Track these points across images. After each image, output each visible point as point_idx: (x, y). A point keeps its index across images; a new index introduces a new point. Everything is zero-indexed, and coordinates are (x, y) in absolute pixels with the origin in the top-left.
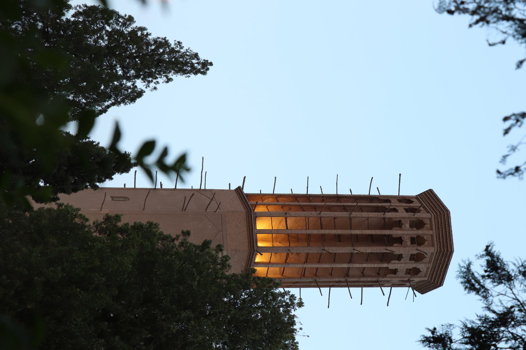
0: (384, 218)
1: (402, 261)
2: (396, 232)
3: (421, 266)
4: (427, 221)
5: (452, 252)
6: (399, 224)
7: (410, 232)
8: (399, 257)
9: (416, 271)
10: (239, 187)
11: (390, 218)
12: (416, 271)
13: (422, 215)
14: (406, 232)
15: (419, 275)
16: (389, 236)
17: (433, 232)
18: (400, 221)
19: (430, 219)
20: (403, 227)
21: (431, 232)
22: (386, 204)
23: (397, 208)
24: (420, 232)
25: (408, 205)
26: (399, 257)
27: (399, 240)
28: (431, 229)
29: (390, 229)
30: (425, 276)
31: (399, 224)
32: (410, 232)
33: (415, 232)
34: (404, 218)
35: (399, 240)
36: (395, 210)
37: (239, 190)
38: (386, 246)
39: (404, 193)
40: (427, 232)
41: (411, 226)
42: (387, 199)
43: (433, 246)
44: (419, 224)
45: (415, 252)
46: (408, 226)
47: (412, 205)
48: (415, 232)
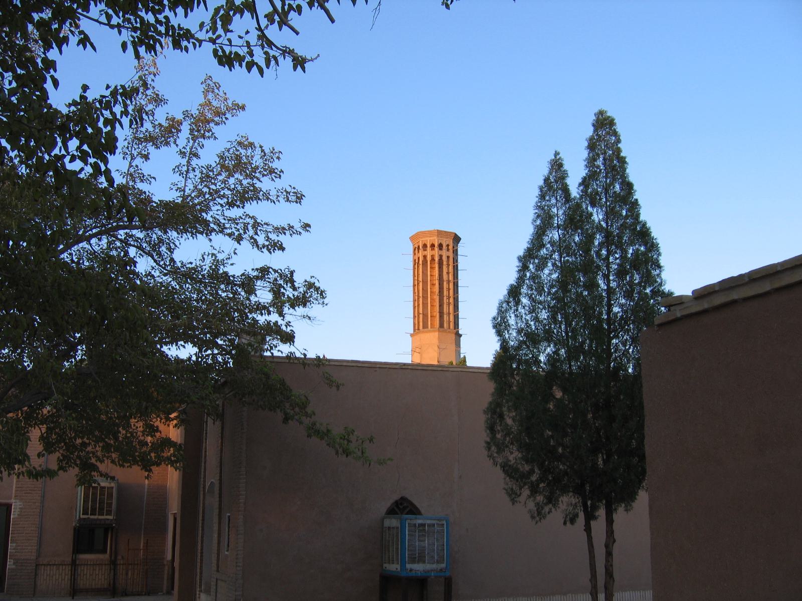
2: (429, 258)
6: (425, 257)
7: (429, 251)
14: (429, 253)
17: (428, 239)
18: (424, 256)
21: (429, 240)
24: (428, 246)
28: (427, 240)
31: (425, 257)
32: (429, 251)
33: (429, 248)
41: (426, 250)
44: (425, 246)
46: (426, 252)
48: (429, 248)
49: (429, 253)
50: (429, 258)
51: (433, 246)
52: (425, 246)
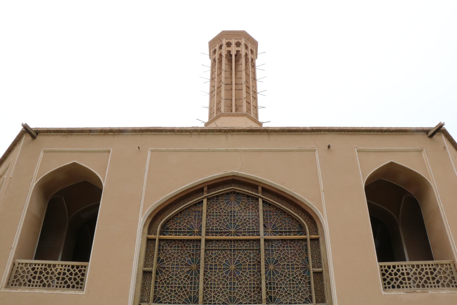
0: (226, 58)
2: (233, 53)
4: (228, 41)
5: (244, 31)
8: (246, 55)
10: (205, 124)
11: (226, 55)
13: (224, 42)
14: (234, 48)
15: (253, 50)
16: (236, 55)
19: (226, 39)
20: (230, 50)
26: (246, 55)
29: (231, 56)
30: (254, 48)
31: (229, 52)
33: (233, 45)
35: (238, 51)
43: (241, 39)
44: (229, 44)
48: (233, 45)
50: (233, 53)
52: (229, 44)
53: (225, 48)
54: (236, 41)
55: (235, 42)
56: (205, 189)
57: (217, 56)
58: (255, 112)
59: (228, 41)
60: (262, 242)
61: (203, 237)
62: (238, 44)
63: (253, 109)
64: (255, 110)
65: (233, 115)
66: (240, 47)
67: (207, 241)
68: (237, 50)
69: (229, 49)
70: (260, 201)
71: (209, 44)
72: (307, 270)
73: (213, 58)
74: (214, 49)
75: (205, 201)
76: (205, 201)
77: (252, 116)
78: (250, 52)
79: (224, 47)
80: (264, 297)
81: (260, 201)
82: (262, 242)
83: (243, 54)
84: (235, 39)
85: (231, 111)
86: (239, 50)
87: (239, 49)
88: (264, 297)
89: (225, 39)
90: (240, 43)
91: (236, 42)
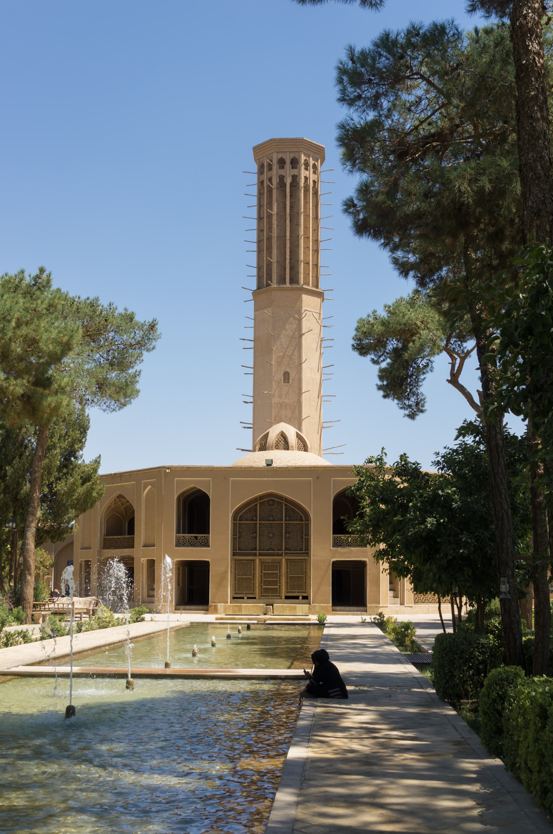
0: (277, 188)
1: (308, 176)
2: (288, 181)
3: (312, 162)
4: (280, 156)
6: (282, 178)
8: (306, 178)
9: (315, 166)
10: (253, 293)
11: (277, 184)
12: (315, 166)
14: (288, 172)
15: (316, 163)
16: (291, 186)
19: (278, 153)
20: (283, 174)
22: (265, 185)
23: (269, 176)
24: (288, 161)
25: (265, 168)
26: (306, 178)
27: (295, 179)
29: (285, 184)
31: (282, 178)
33: (288, 165)
34: (277, 172)
36: (270, 180)
37: (255, 293)
38: (299, 188)
39: (256, 170)
40: (288, 156)
42: (261, 183)
44: (282, 163)
45: (303, 167)
47: (265, 165)
48: (288, 165)
49: (288, 172)
50: (288, 181)
51: (307, 164)
53: (277, 170)
54: (292, 155)
55: (290, 157)
56: (258, 499)
57: (265, 177)
58: (315, 275)
59: (280, 157)
60: (284, 524)
61: (258, 522)
62: (295, 163)
63: (313, 268)
64: (315, 270)
65: (287, 289)
66: (296, 168)
67: (260, 523)
68: (293, 174)
69: (282, 172)
70: (284, 505)
71: (254, 151)
72: (302, 538)
73: (261, 180)
74: (261, 164)
75: (258, 505)
76: (258, 505)
77: (310, 287)
78: (312, 170)
79: (275, 167)
80: (284, 548)
81: (284, 505)
82: (284, 524)
83: (302, 184)
84: (290, 152)
85: (285, 283)
86: (296, 174)
87: (295, 172)
88: (284, 548)
89: (276, 153)
90: (297, 159)
91: (292, 158)
